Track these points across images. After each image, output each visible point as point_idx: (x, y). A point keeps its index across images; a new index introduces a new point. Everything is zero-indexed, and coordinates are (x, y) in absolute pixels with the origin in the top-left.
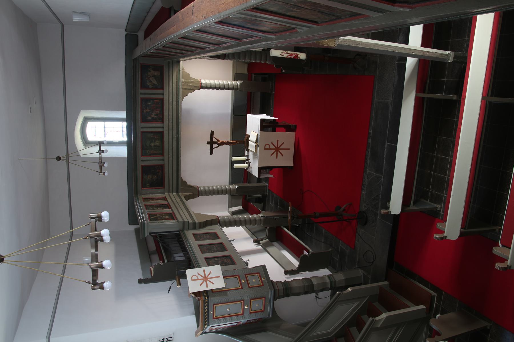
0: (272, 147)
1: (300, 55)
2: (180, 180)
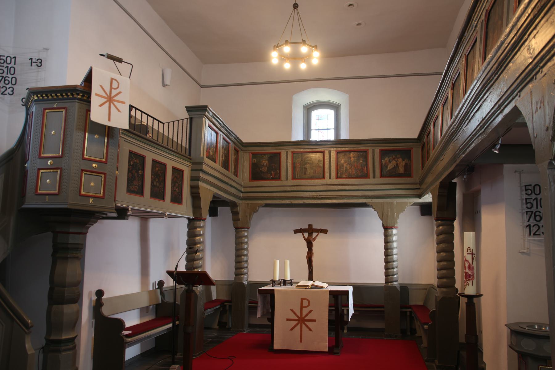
0: (305, 311)
1: (472, 285)
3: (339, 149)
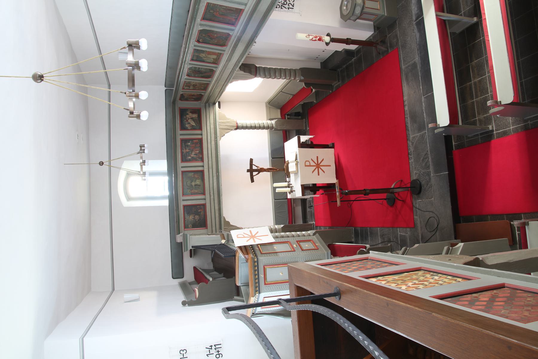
0: (312, 164)
2: (222, 220)
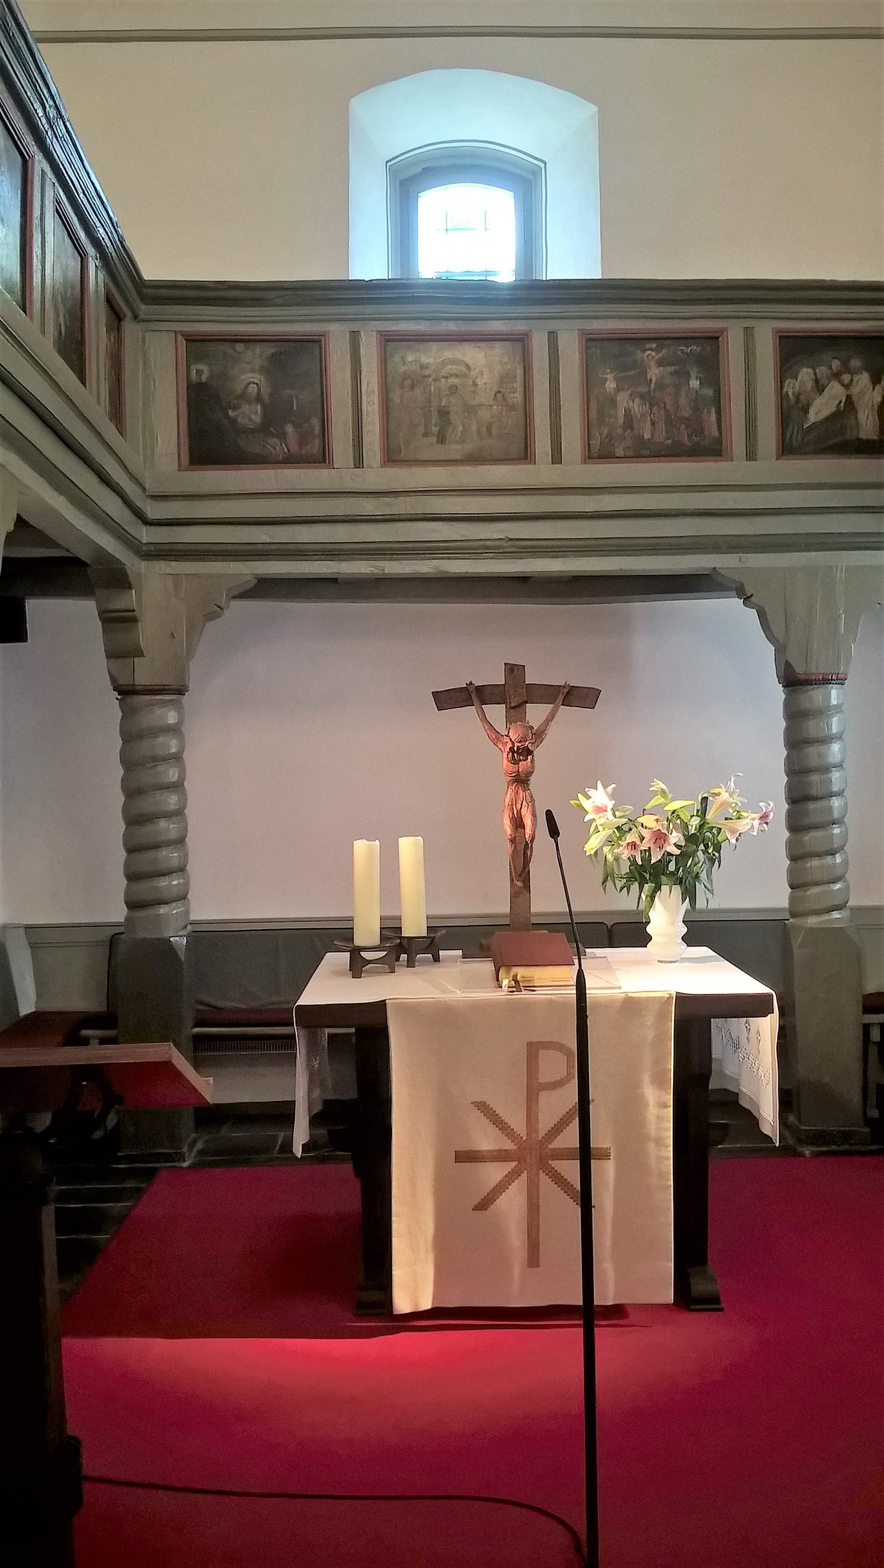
3: (596, 325)
